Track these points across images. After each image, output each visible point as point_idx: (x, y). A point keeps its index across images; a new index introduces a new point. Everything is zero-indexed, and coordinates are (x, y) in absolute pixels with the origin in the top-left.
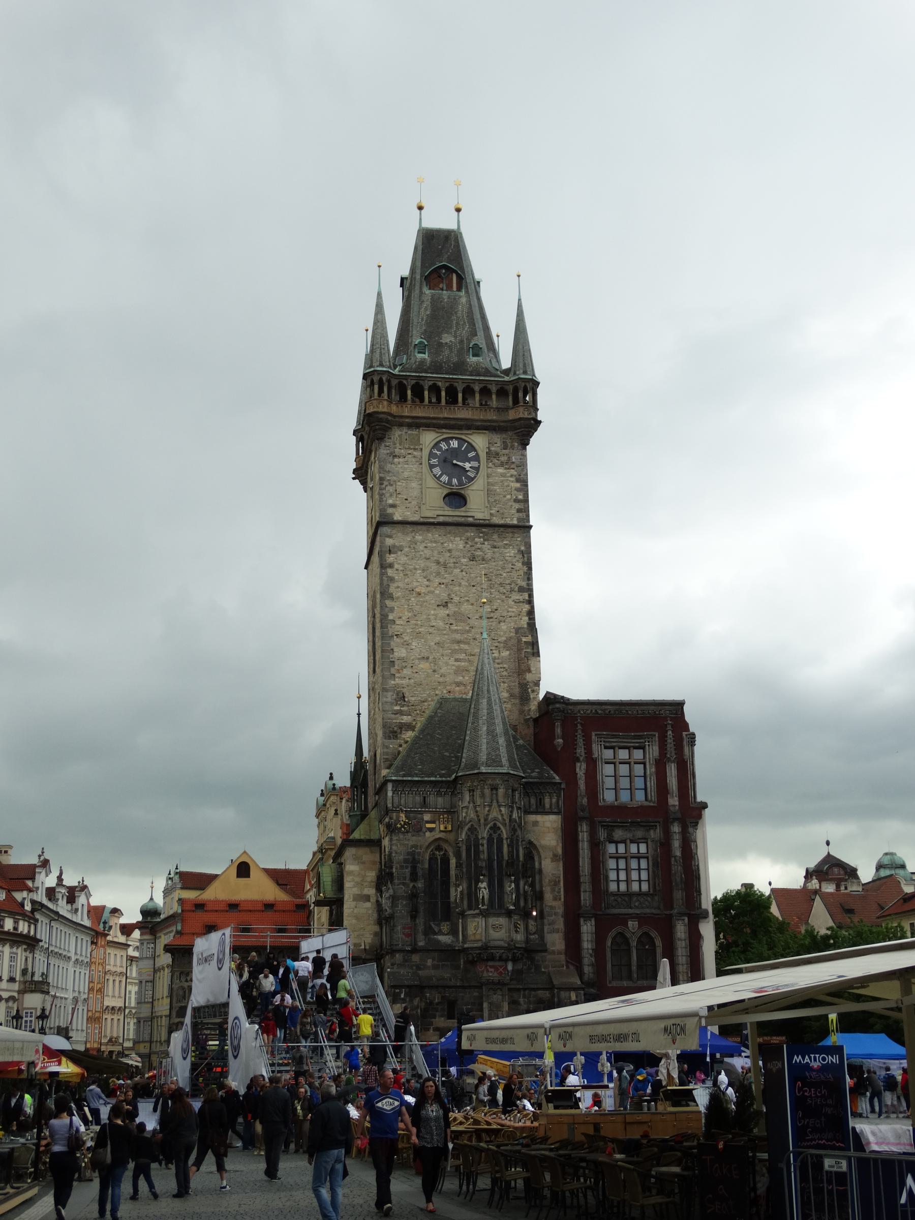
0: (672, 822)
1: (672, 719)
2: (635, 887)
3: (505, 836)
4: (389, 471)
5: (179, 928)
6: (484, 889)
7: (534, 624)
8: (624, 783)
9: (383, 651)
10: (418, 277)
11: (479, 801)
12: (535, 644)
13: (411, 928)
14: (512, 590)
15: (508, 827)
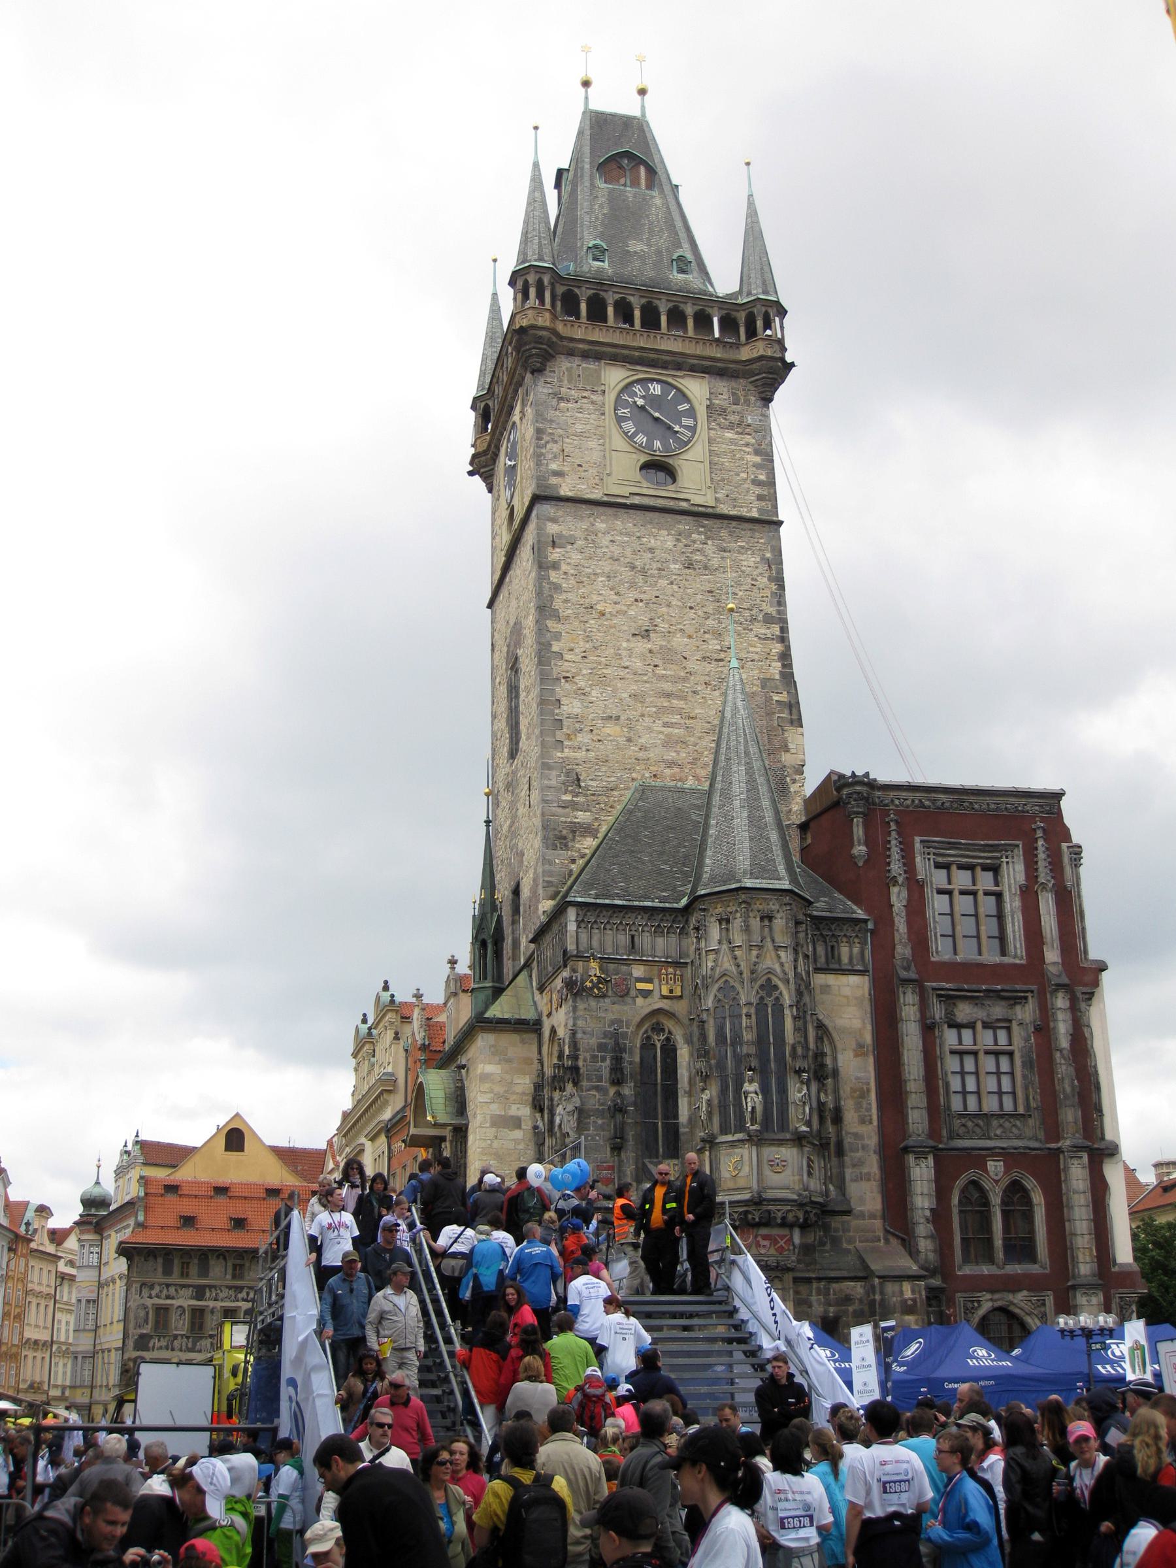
0: (1056, 990)
1: (1043, 820)
2: (990, 1105)
3: (787, 1000)
4: (551, 421)
5: (141, 1218)
6: (752, 1095)
7: (792, 673)
8: (966, 926)
9: (542, 702)
10: (587, 166)
11: (738, 939)
12: (793, 706)
13: (611, 1168)
14: (753, 620)
15: (792, 986)
